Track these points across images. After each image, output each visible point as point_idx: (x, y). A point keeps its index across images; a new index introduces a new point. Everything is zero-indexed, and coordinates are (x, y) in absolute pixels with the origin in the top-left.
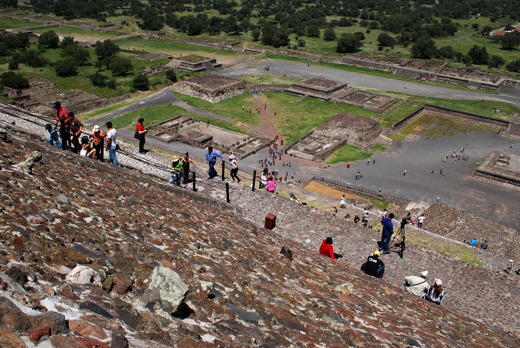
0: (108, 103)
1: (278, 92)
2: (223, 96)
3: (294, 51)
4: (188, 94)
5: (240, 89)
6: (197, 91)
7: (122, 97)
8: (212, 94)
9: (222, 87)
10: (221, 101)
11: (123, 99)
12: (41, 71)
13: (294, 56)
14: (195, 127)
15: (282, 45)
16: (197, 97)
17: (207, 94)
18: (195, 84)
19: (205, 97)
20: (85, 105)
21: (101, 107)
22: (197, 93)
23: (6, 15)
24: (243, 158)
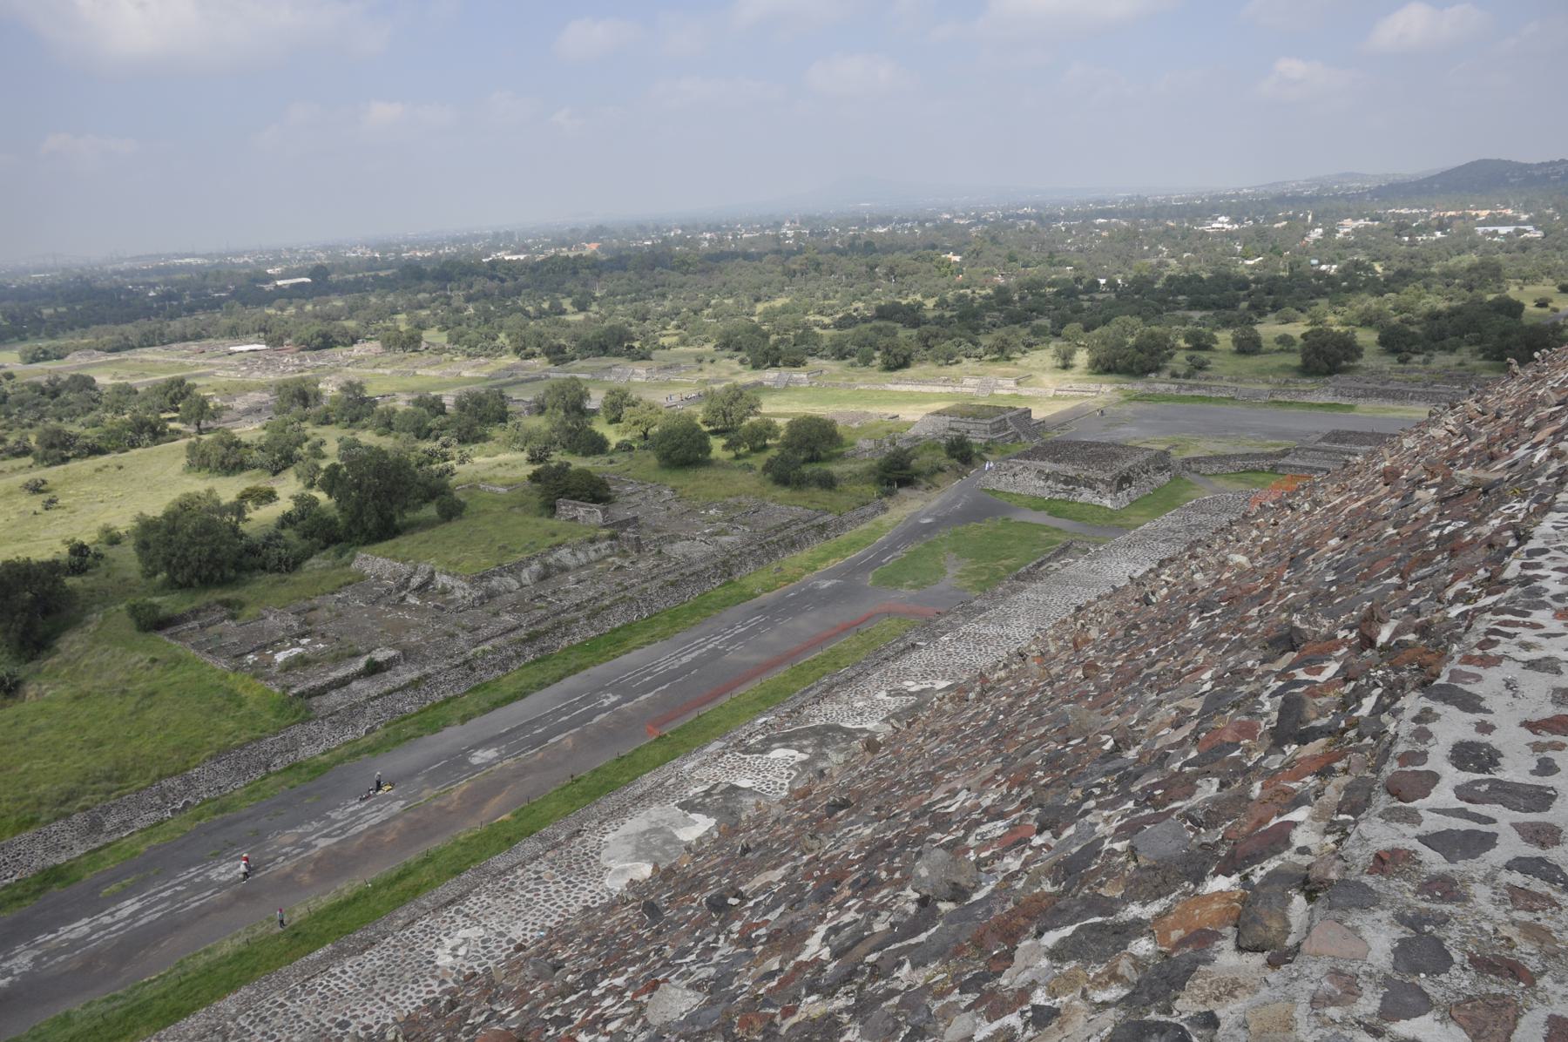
0: (842, 526)
1: (1255, 471)
2: (1133, 490)
3: (1190, 381)
4: (1031, 490)
5: (1160, 469)
6: (1057, 481)
7: (869, 510)
8: (1108, 484)
10: (1132, 502)
11: (872, 515)
12: (611, 462)
13: (1196, 392)
15: (1150, 371)
16: (1064, 496)
18: (1048, 466)
19: (1086, 495)
21: (828, 538)
22: (1060, 486)
23: (402, 367)
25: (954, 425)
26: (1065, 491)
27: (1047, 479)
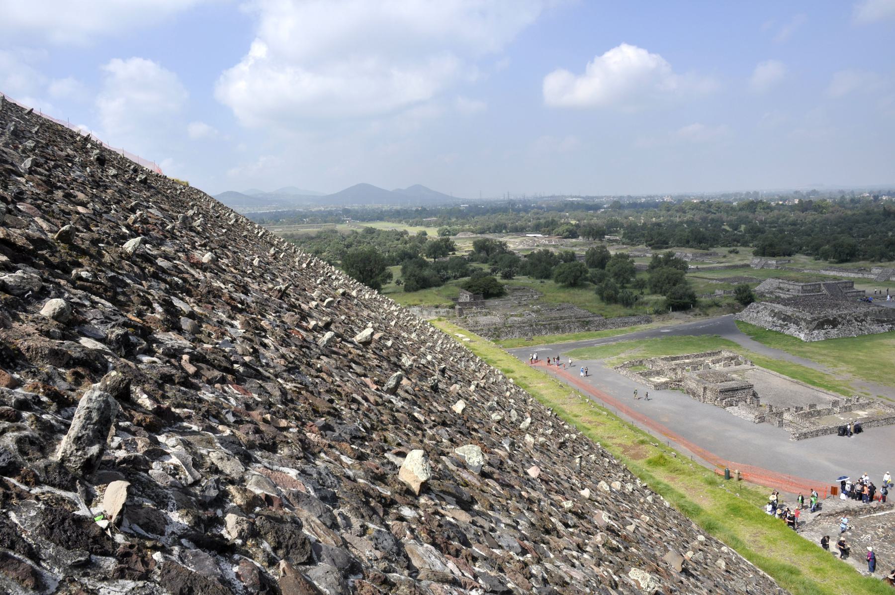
2: (835, 331)
4: (763, 323)
5: (880, 322)
6: (780, 318)
7: (634, 319)
9: (832, 313)
11: (635, 323)
14: (735, 372)
16: (778, 329)
17: (798, 325)
19: (792, 330)
20: (560, 322)
21: (589, 330)
22: (780, 322)
24: (806, 435)
25: (781, 285)
26: (781, 326)
27: (774, 316)
